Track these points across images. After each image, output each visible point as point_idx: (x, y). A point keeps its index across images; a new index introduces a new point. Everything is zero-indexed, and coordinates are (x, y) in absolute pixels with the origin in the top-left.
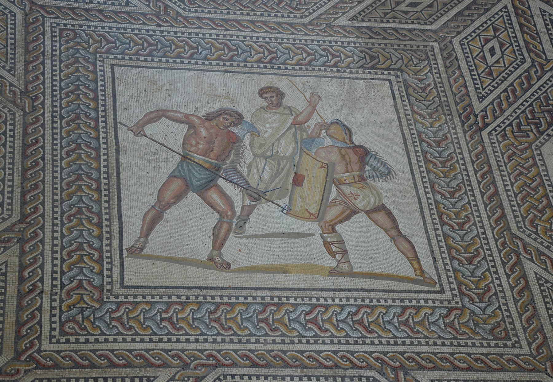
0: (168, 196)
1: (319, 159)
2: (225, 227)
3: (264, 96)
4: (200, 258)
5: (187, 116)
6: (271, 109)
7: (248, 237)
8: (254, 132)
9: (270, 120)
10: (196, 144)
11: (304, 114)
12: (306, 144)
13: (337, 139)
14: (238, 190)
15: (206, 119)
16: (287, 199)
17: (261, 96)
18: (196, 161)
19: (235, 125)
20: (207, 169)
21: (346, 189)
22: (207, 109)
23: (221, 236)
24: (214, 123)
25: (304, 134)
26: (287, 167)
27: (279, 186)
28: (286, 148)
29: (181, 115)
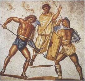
0: (12, 52)
1: (58, 35)
2: (27, 63)
3: (44, 8)
4: (19, 75)
5: (19, 19)
6: (46, 14)
7: (33, 67)
8: (39, 25)
9: (45, 19)
10: (21, 31)
11: (56, 15)
12: (55, 29)
13: (65, 26)
14: (32, 49)
15: (25, 20)
16: (46, 52)
17: (43, 9)
18: (21, 38)
19: (34, 22)
20: (23, 41)
21: (65, 47)
22: (25, 15)
23: (26, 66)
24: (27, 22)
25: (55, 24)
26: (48, 39)
27: (44, 47)
28: (48, 31)
29: (17, 19)
